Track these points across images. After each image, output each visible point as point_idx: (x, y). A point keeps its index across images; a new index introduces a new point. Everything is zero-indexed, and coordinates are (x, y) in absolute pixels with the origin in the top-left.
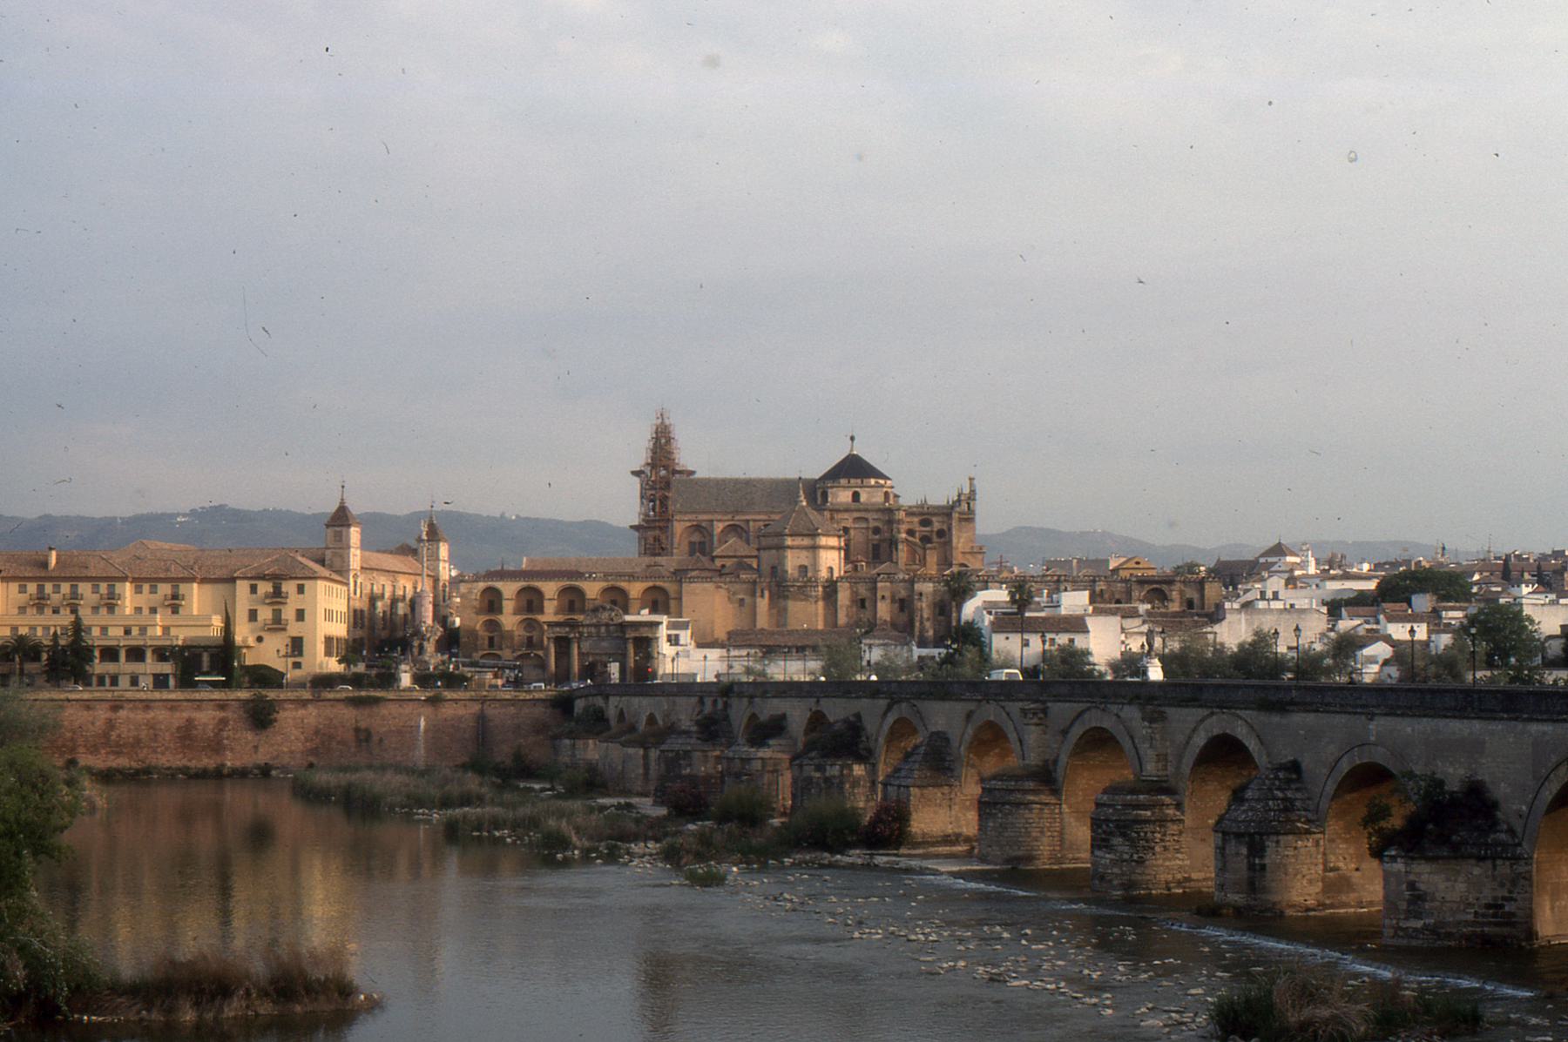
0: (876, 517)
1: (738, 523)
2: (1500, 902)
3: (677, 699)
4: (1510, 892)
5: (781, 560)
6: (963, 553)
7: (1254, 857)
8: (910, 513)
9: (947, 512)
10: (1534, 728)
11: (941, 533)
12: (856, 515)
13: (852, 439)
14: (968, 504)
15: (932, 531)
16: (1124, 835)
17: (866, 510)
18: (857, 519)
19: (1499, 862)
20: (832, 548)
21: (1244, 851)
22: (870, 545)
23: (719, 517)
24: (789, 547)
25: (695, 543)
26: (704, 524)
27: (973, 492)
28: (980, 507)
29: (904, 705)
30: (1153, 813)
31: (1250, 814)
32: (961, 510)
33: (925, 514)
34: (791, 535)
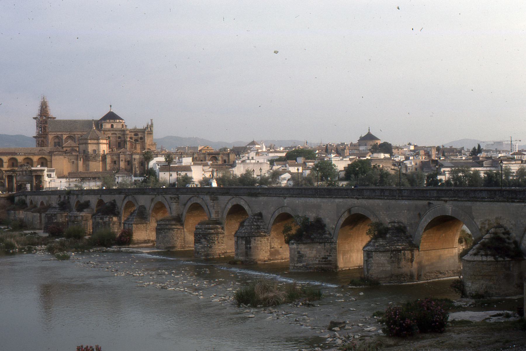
0: (119, 133)
1: (71, 135)
2: (327, 257)
3: (52, 196)
4: (330, 253)
5: (87, 148)
6: (149, 145)
7: (247, 244)
8: (131, 132)
9: (143, 131)
10: (337, 200)
11: (141, 138)
12: (112, 132)
13: (111, 106)
14: (150, 128)
15: (138, 138)
16: (205, 238)
17: (116, 131)
18: (112, 134)
19: (326, 244)
20: (104, 144)
21: (244, 242)
22: (117, 143)
23: (65, 133)
24: (89, 143)
25: (56, 142)
26: (59, 136)
27: (152, 124)
28: (155, 130)
29: (130, 197)
30: (214, 231)
31: (246, 230)
32: (148, 130)
33: (136, 132)
34: (90, 139)
